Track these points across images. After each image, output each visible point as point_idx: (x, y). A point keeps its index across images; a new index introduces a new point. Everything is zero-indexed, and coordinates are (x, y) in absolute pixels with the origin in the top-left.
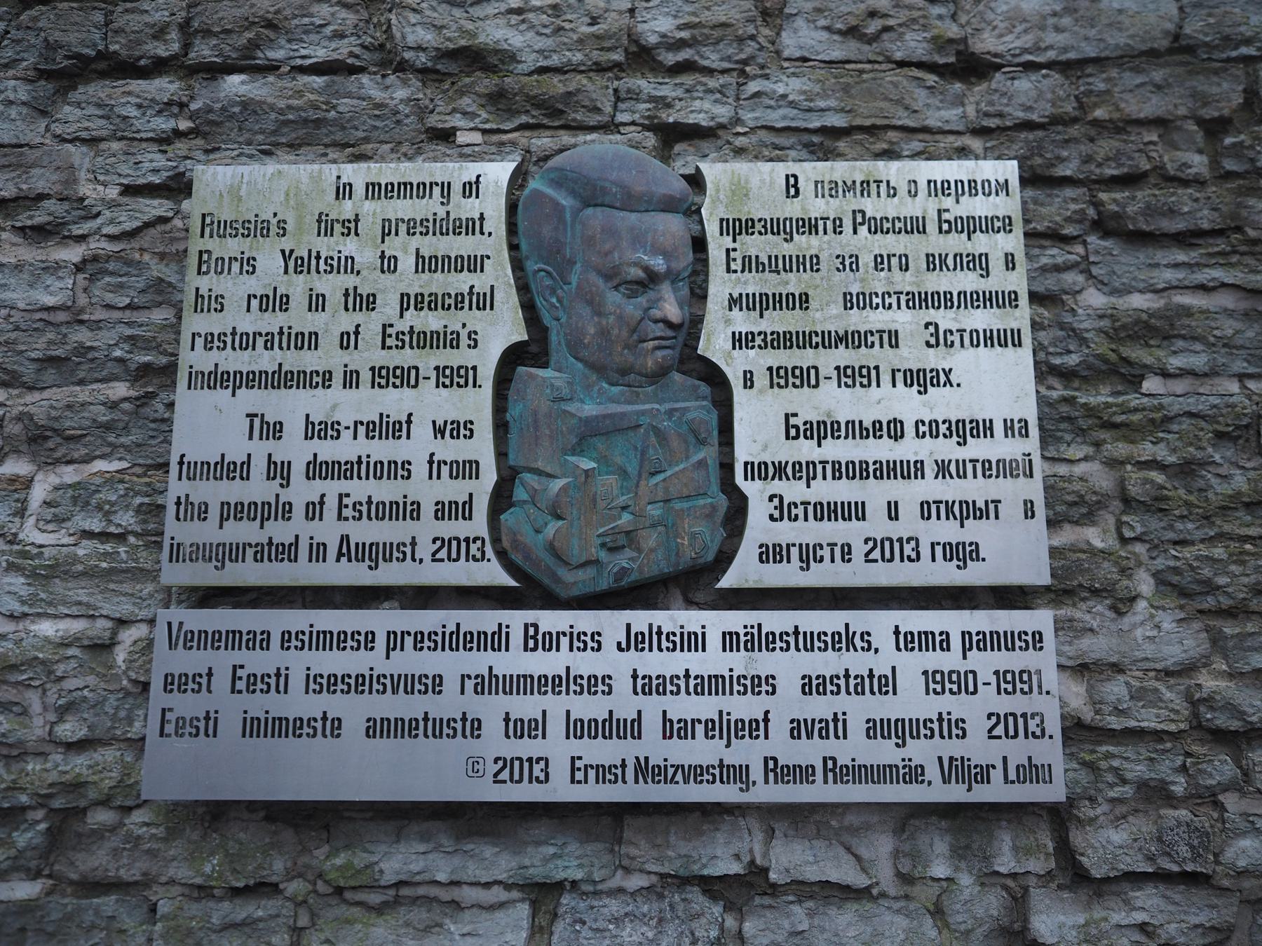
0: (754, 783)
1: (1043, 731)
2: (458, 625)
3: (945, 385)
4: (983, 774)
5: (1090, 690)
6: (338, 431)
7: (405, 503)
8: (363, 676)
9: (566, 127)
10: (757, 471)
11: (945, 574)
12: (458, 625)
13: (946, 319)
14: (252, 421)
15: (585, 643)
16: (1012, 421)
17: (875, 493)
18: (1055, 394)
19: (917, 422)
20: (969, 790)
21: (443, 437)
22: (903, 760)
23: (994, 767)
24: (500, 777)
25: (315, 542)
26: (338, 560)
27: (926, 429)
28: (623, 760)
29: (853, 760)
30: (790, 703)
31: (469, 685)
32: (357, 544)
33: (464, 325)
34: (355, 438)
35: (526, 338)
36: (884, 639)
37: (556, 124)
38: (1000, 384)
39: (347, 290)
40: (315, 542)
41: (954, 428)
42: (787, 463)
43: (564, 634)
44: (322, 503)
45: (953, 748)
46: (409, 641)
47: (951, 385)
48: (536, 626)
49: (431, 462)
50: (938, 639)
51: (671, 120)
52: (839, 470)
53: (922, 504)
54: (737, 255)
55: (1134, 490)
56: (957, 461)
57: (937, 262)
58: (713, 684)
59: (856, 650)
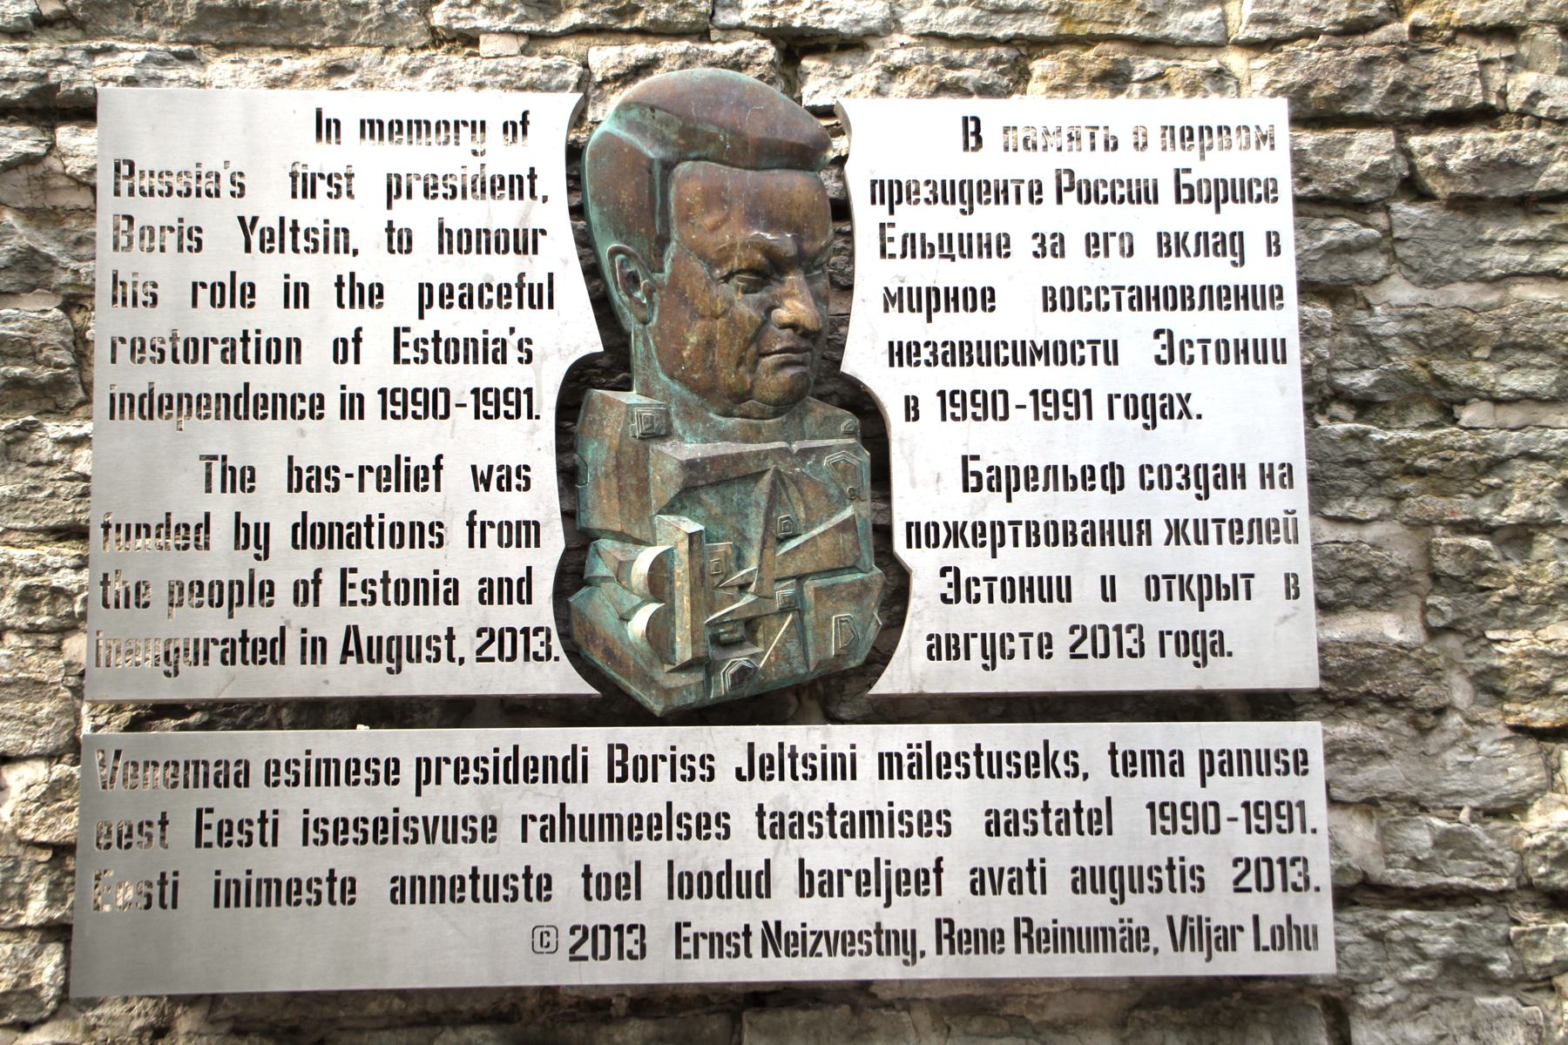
0: (923, 954)
1: (1307, 881)
2: (516, 748)
3: (1180, 417)
4: (1227, 938)
5: (1383, 832)
6: (336, 480)
7: (436, 581)
8: (385, 820)
9: (642, 32)
10: (922, 534)
11: (1179, 675)
12: (516, 748)
13: (1186, 324)
14: (209, 466)
15: (692, 769)
16: (1271, 465)
17: (1083, 565)
18: (1340, 427)
19: (1142, 468)
20: (1209, 959)
21: (487, 489)
22: (1122, 921)
23: (1241, 929)
24: (579, 953)
25: (309, 636)
26: (343, 662)
27: (1154, 477)
28: (747, 927)
29: (1055, 921)
30: (968, 847)
31: (534, 828)
32: (370, 639)
33: (512, 330)
34: (361, 489)
35: (600, 348)
36: (1095, 759)
37: (626, 26)
38: (1256, 415)
39: (340, 277)
40: (309, 636)
41: (1192, 476)
42: (965, 524)
43: (663, 758)
44: (317, 582)
45: (1186, 904)
46: (448, 771)
47: (1189, 417)
48: (624, 748)
49: (471, 524)
50: (1168, 760)
51: (797, 23)
52: (1036, 534)
53: (1148, 579)
54: (896, 233)
55: (1445, 564)
56: (1196, 521)
57: (1173, 244)
58: (869, 823)
59: (1058, 775)
